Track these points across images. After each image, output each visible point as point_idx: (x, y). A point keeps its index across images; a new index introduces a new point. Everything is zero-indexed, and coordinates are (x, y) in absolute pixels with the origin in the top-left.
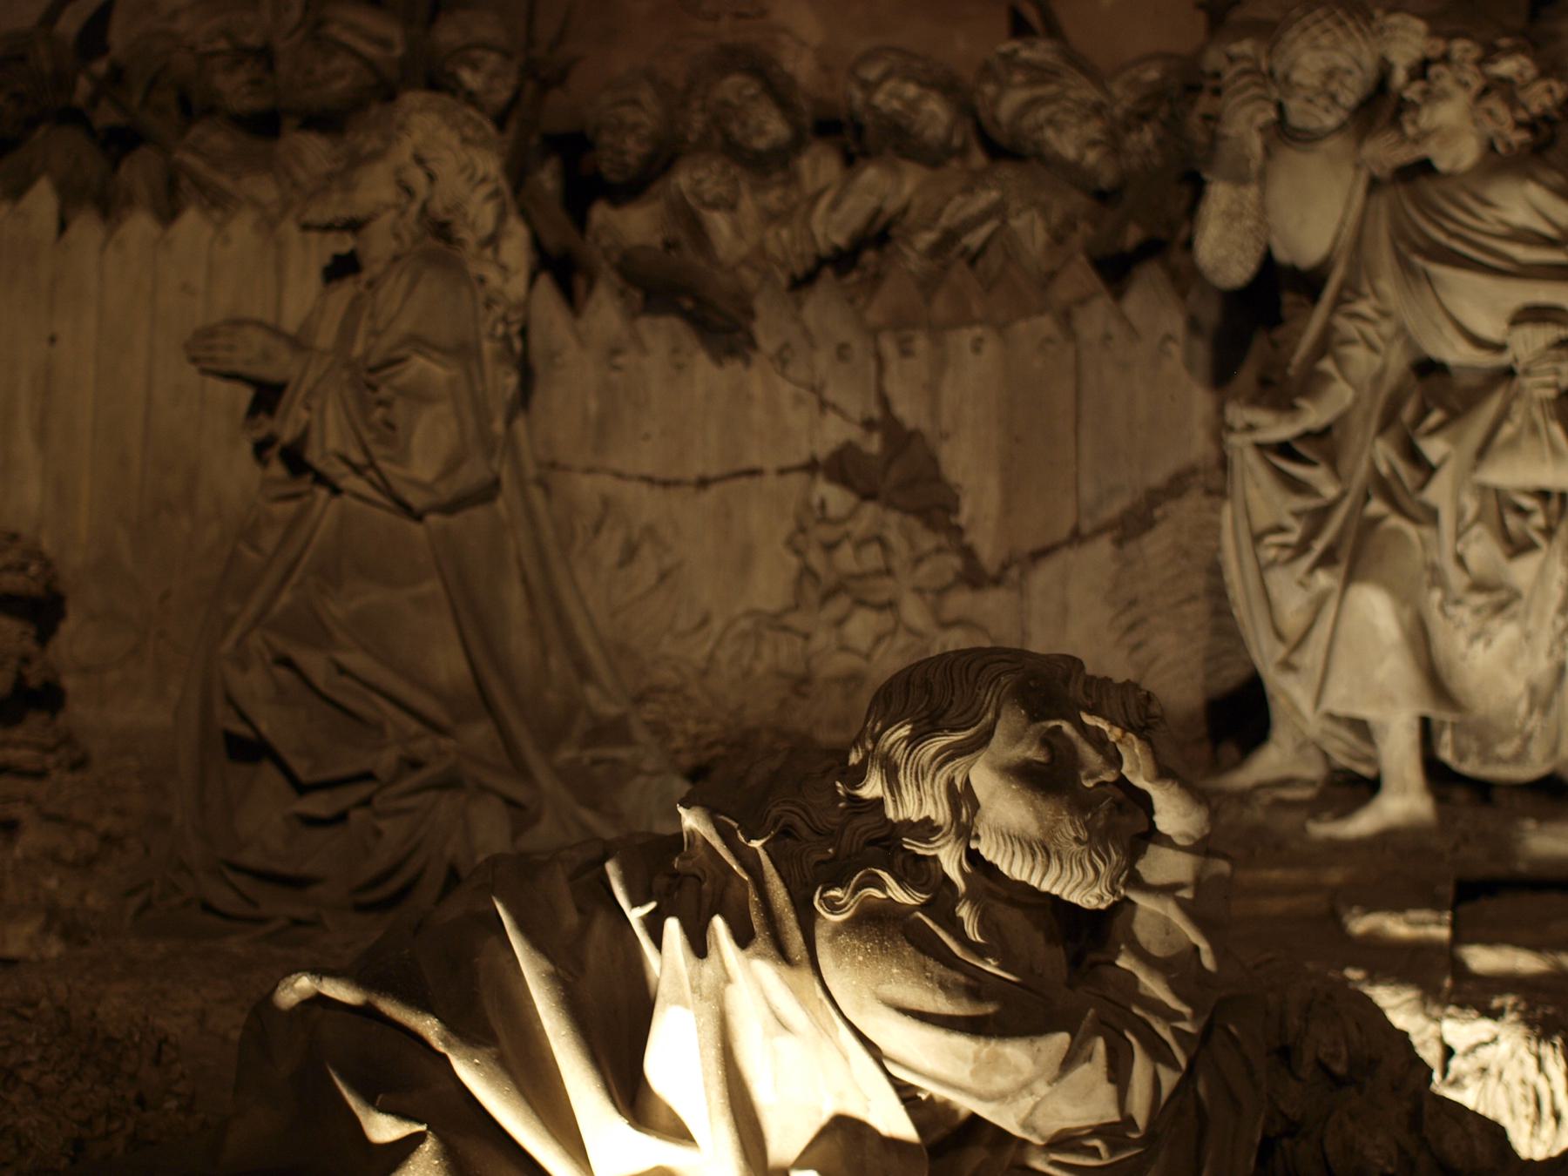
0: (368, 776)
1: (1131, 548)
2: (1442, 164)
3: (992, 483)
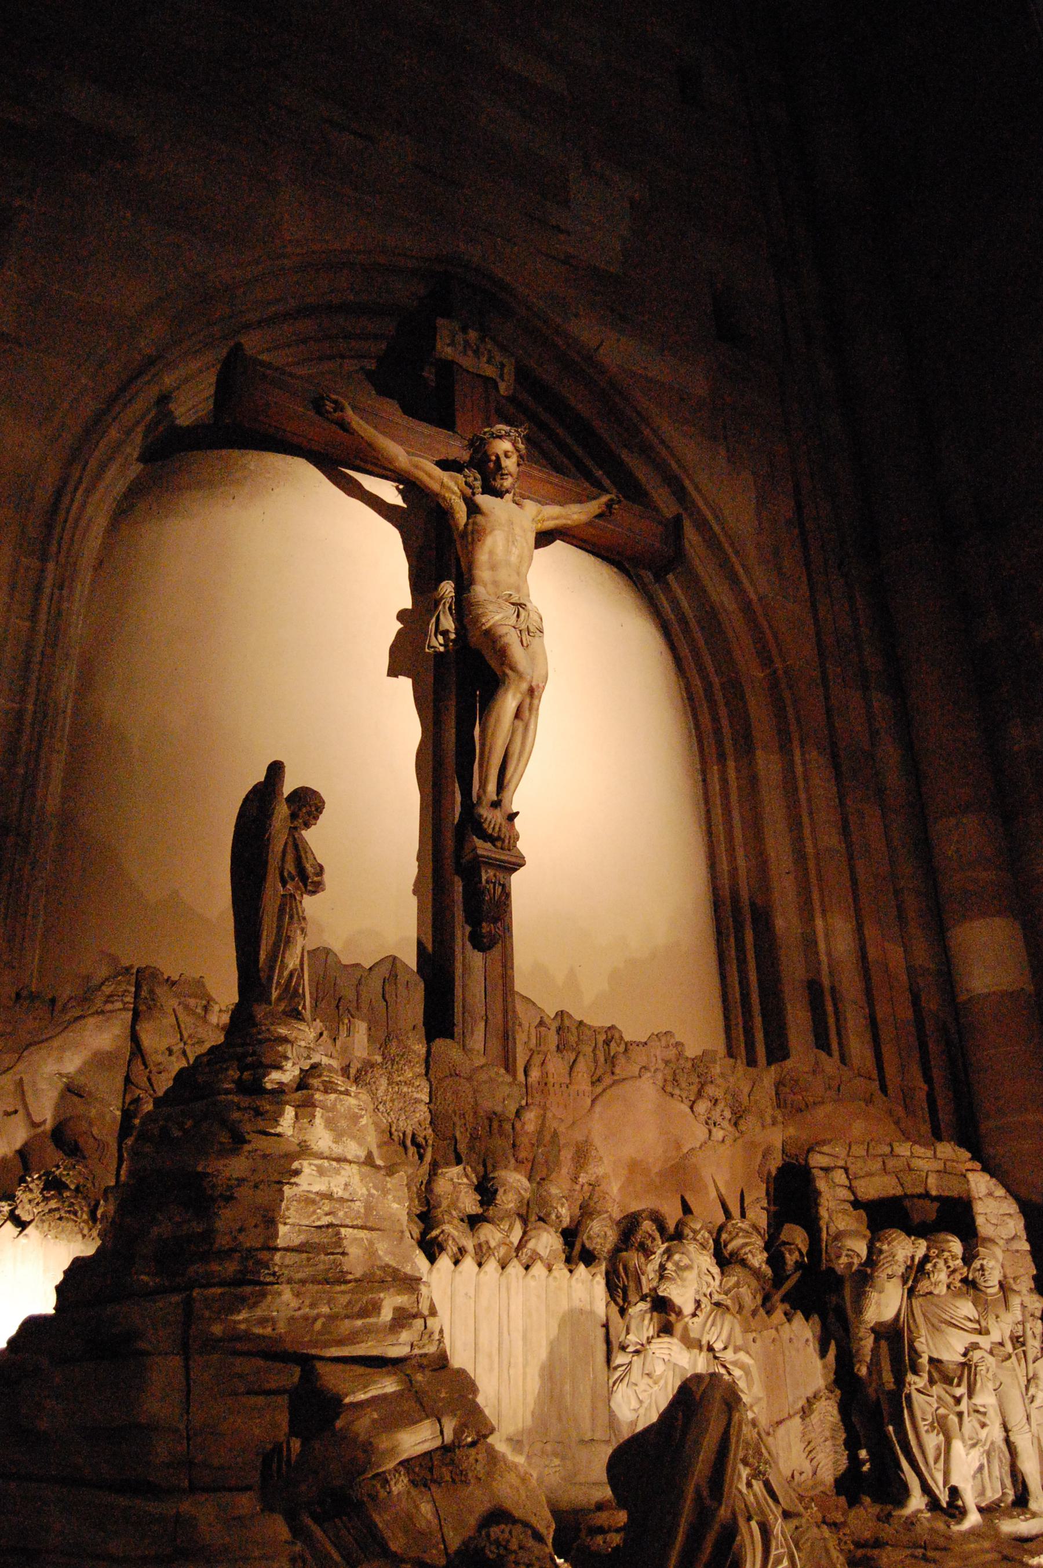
1: (808, 1419)
2: (936, 1292)
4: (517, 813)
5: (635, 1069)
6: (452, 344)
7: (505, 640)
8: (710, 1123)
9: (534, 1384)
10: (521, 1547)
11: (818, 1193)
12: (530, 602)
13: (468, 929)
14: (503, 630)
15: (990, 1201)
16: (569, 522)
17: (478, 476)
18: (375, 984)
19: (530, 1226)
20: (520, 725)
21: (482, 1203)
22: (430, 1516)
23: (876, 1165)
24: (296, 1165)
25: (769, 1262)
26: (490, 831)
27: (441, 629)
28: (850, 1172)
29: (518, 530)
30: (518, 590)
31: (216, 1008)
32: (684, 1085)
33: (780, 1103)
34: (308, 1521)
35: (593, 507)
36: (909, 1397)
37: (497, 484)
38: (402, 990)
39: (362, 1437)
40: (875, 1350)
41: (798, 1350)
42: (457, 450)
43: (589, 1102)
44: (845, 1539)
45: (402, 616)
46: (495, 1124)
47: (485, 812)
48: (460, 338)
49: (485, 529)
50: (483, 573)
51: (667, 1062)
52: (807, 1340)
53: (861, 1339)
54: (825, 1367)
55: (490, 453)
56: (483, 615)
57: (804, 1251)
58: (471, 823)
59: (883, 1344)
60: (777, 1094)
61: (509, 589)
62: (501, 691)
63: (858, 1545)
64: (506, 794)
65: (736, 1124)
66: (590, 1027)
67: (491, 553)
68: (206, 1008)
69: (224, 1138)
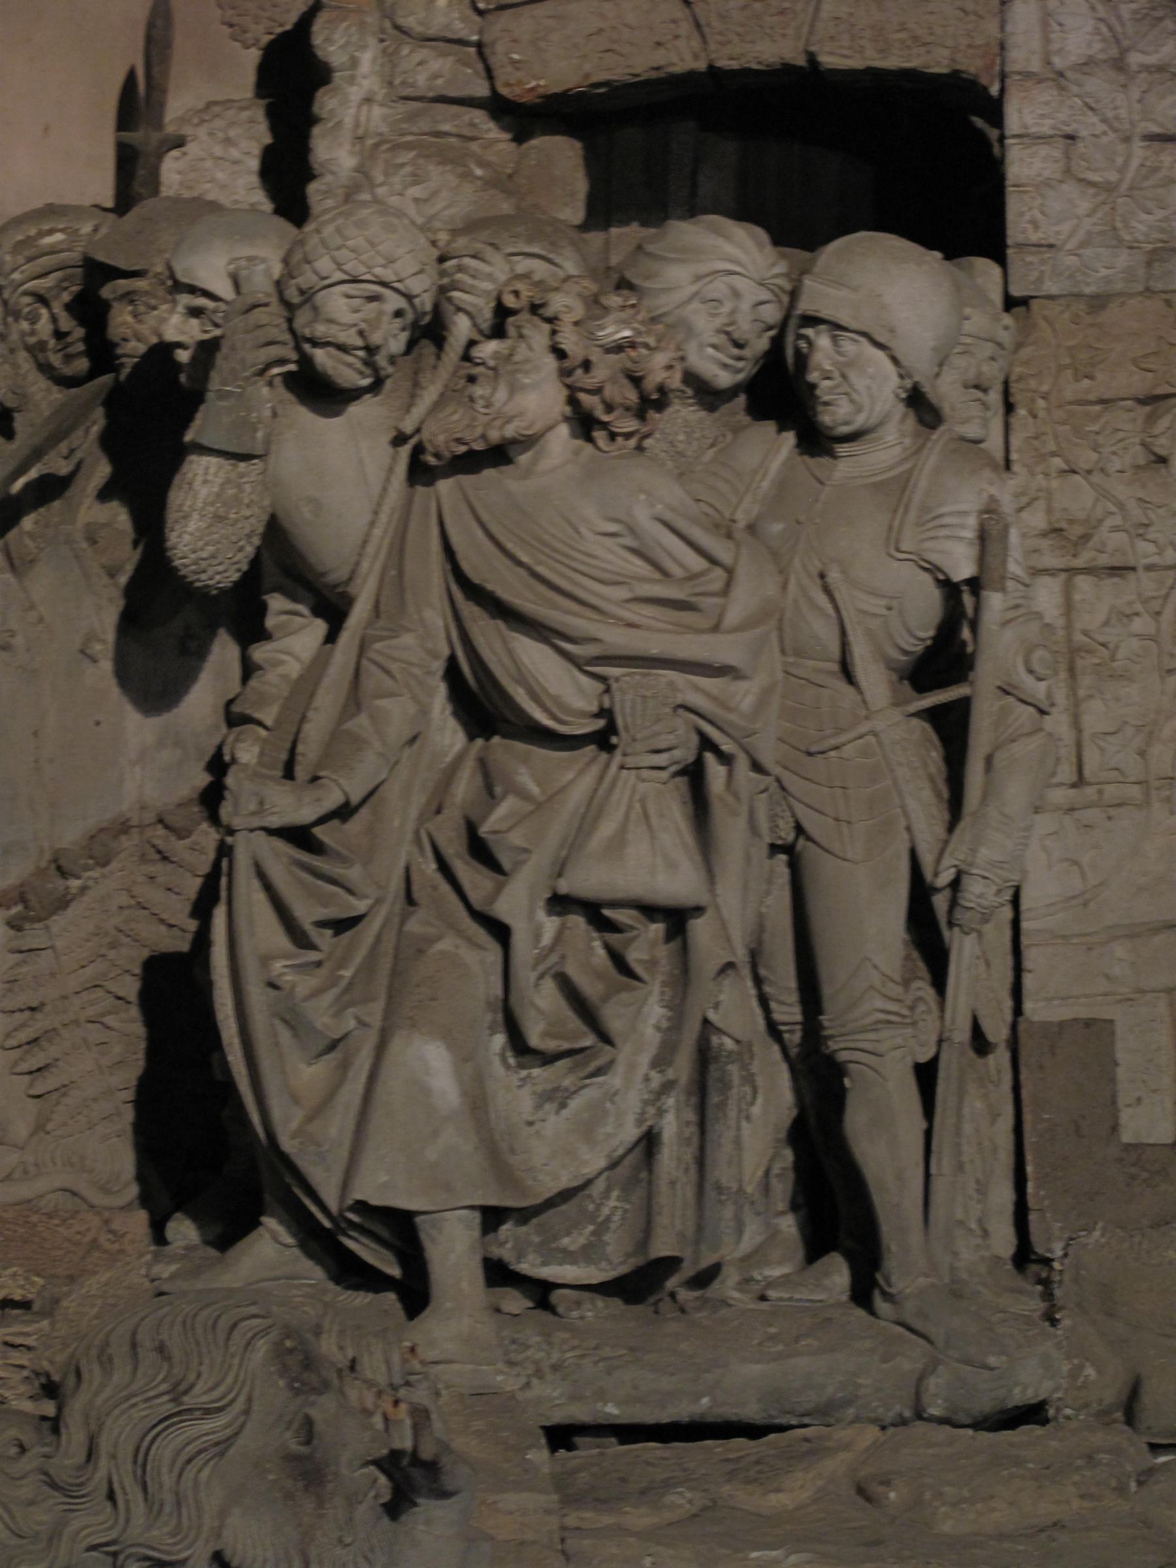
15: (1097, 85)
52: (91, 637)
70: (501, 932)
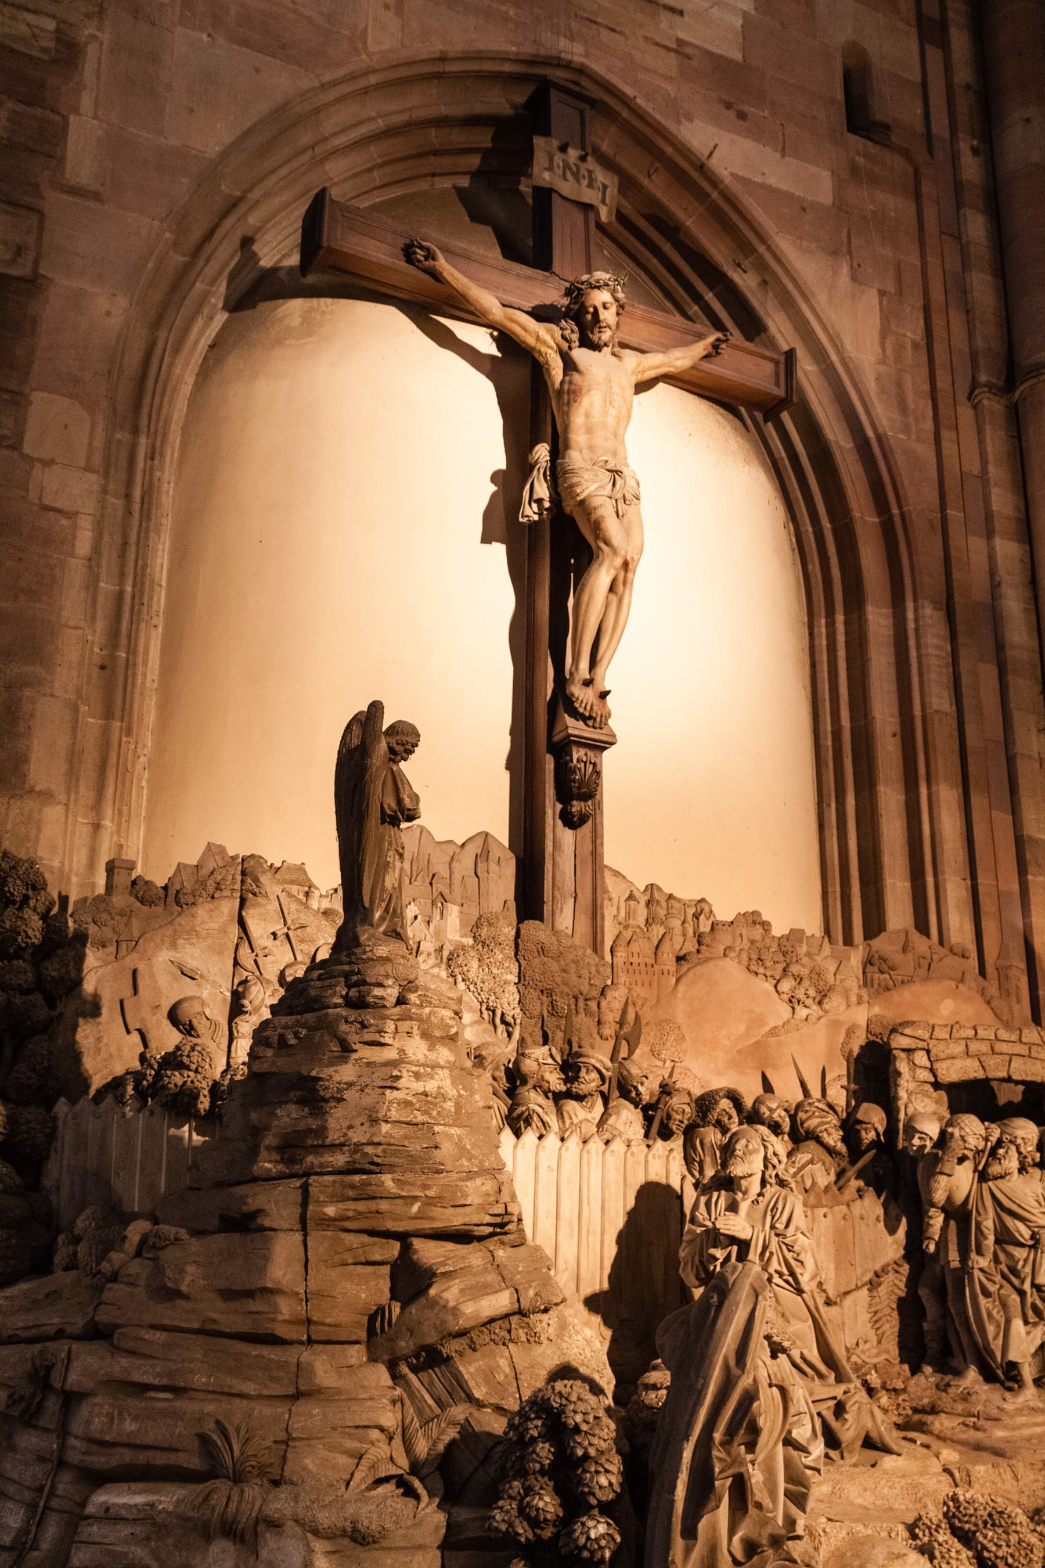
0: (834, 1398)
1: (875, 1294)
3: (832, 1266)
4: (609, 692)
5: (722, 948)
6: (550, 169)
7: (600, 512)
8: (792, 1001)
9: (611, 1250)
10: (580, 1399)
11: (899, 1074)
12: (627, 465)
13: (559, 806)
14: (596, 502)
16: (672, 369)
17: (576, 328)
18: (467, 860)
19: (612, 1104)
20: (614, 599)
21: (566, 1081)
22: (507, 1370)
23: (959, 1048)
24: (395, 1073)
25: (844, 1140)
26: (581, 710)
27: (535, 497)
28: (932, 1054)
29: (616, 389)
30: (615, 454)
31: (317, 893)
32: (768, 964)
33: (866, 983)
34: (404, 1369)
35: (700, 349)
36: (971, 1276)
37: (595, 338)
38: (493, 866)
39: (452, 1304)
40: (944, 1229)
41: (868, 1225)
42: (553, 295)
43: (673, 981)
44: (903, 1404)
45: (495, 477)
46: (581, 1003)
47: (577, 690)
48: (558, 159)
49: (581, 389)
50: (578, 437)
51: (753, 942)
53: (931, 1218)
54: (896, 1242)
55: (587, 304)
56: (577, 484)
57: (881, 1130)
58: (563, 700)
59: (952, 1223)
60: (864, 973)
61: (605, 454)
62: (595, 566)
63: (915, 1410)
64: (599, 671)
65: (820, 1003)
66: (679, 900)
67: (587, 415)
68: (307, 894)
69: (335, 1048)
70: (1022, 1293)
